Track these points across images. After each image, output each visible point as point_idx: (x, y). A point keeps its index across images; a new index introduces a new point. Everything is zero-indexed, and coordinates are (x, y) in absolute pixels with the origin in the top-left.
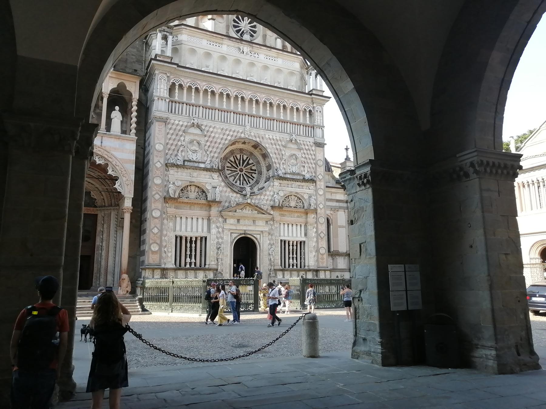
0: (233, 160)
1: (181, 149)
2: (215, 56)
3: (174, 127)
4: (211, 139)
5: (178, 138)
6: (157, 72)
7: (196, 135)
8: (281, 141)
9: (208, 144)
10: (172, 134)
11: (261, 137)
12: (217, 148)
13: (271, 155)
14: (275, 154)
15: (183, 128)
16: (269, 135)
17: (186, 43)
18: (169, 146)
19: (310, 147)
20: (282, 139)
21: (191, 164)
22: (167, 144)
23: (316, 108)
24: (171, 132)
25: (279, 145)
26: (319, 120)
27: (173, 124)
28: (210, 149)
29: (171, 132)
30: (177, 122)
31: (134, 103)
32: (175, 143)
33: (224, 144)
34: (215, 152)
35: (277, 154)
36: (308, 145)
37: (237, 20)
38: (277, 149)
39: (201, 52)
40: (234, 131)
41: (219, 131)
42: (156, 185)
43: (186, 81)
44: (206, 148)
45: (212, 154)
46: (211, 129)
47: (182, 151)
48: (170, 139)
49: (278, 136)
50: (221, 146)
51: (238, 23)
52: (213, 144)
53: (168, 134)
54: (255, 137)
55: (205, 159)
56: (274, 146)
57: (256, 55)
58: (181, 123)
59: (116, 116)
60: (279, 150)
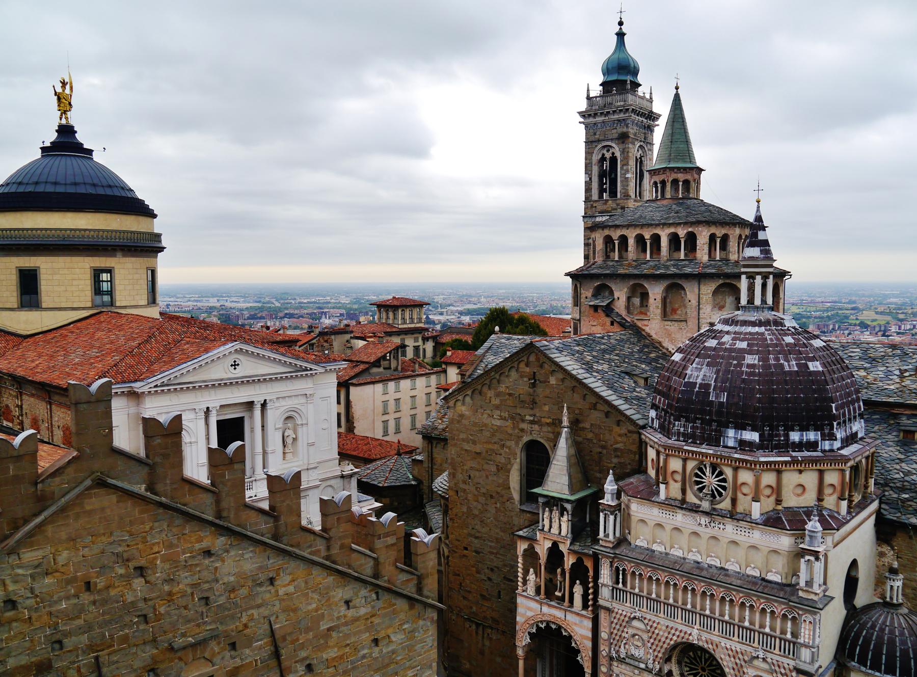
0: (688, 661)
1: (624, 642)
2: (668, 528)
3: (618, 616)
4: (654, 636)
5: (621, 629)
6: (600, 557)
7: (638, 629)
8: (742, 654)
9: (652, 641)
10: (616, 624)
11: (714, 645)
12: (662, 647)
13: (727, 670)
14: (734, 669)
15: (627, 619)
16: (724, 642)
17: (635, 514)
18: (613, 636)
19: (788, 672)
20: (744, 652)
21: (632, 662)
22: (612, 633)
23: (804, 616)
24: (615, 621)
25: (739, 659)
26: (807, 636)
27: (617, 613)
28: (654, 647)
29: (615, 621)
30: (620, 612)
31: (590, 580)
32: (619, 633)
33: (669, 644)
34: (659, 652)
35: (736, 670)
36: (784, 668)
37: (699, 473)
38: (736, 664)
39: (651, 523)
40: (681, 631)
41: (664, 628)
42: (603, 673)
43: (629, 566)
44: (649, 645)
45: (656, 653)
46: (655, 625)
47: (625, 644)
48: (614, 628)
49: (739, 647)
50: (665, 646)
51: (703, 478)
52: (656, 642)
53: (612, 622)
54: (707, 642)
55: (649, 656)
56: (732, 659)
57: (722, 526)
58: (624, 613)
59: (578, 590)
60: (739, 665)
